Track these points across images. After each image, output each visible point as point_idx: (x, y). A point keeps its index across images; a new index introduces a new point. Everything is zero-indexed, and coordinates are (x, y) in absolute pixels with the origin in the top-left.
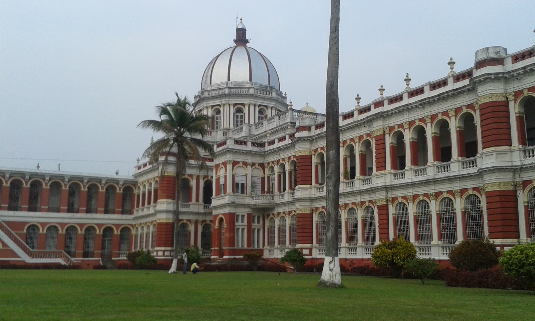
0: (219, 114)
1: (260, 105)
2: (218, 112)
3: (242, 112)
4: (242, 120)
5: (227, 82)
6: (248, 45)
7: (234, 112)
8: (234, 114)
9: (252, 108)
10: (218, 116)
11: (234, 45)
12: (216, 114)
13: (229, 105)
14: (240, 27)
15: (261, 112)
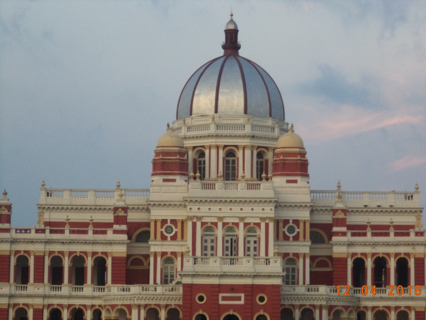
0: (203, 157)
1: (259, 147)
2: (202, 154)
3: (234, 156)
4: (235, 167)
5: (213, 116)
6: (242, 53)
7: (224, 156)
8: (224, 159)
9: (248, 152)
10: (202, 159)
11: (221, 52)
12: (199, 157)
13: (218, 147)
14: (231, 27)
15: (260, 155)
